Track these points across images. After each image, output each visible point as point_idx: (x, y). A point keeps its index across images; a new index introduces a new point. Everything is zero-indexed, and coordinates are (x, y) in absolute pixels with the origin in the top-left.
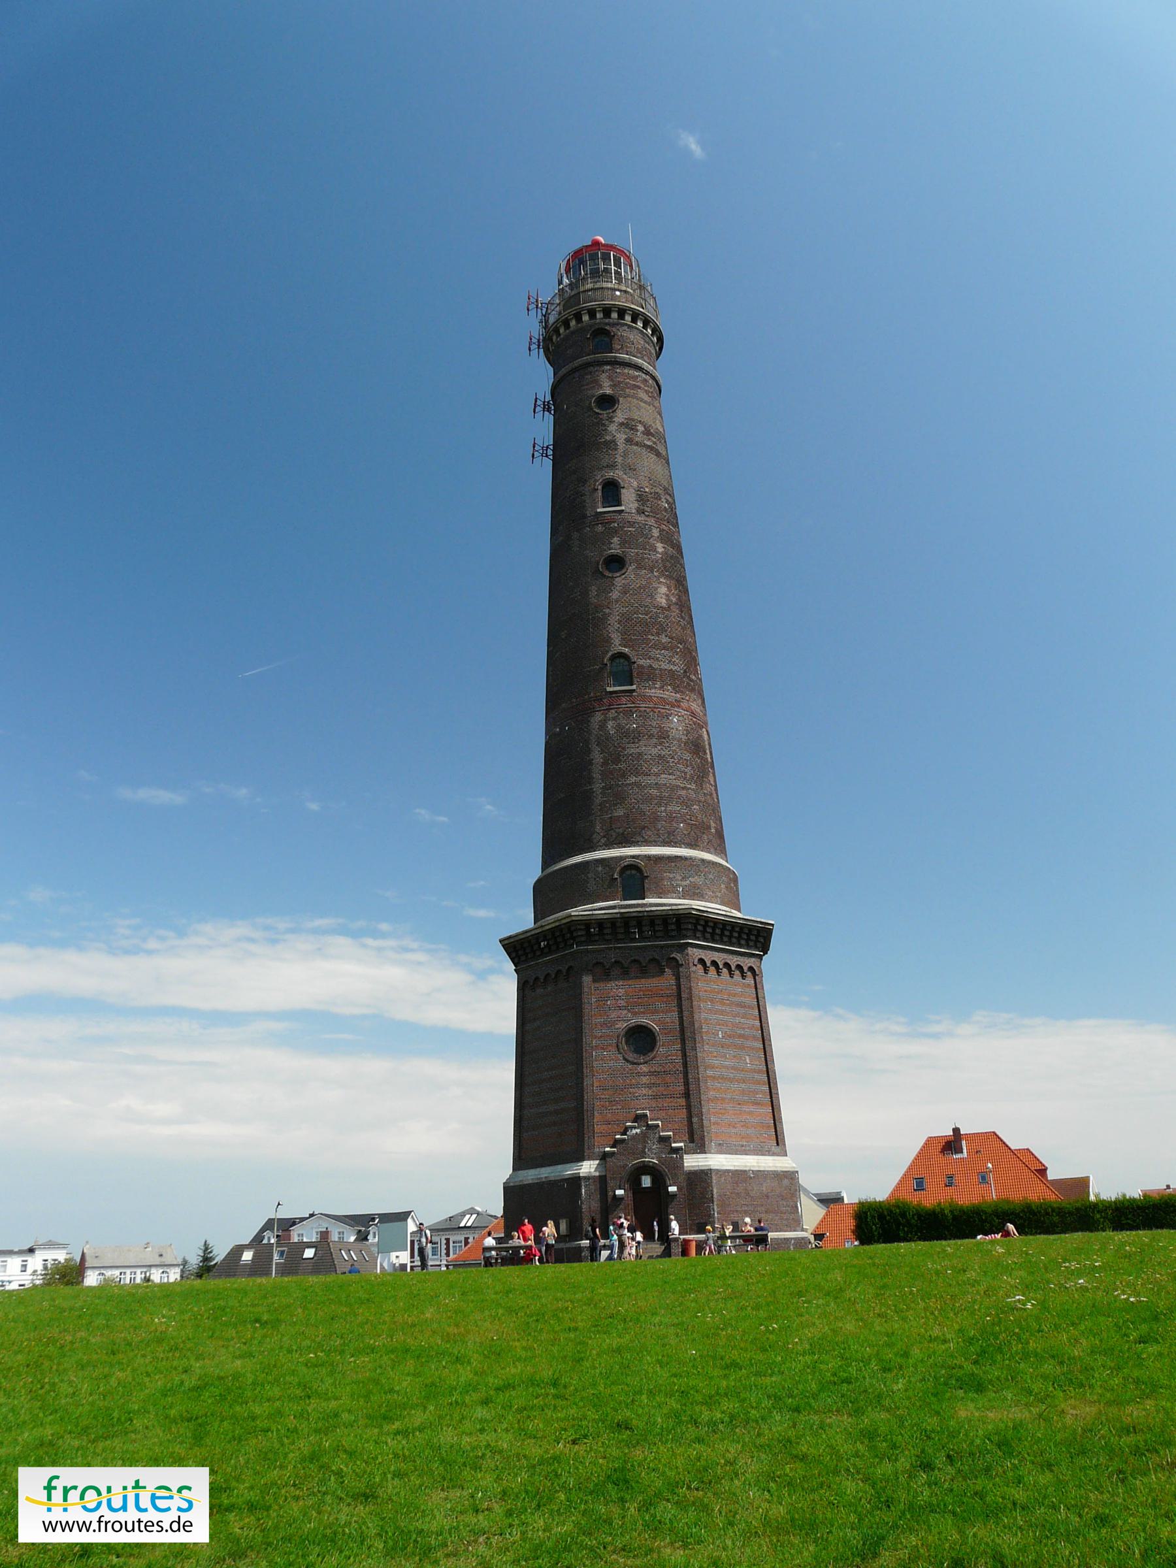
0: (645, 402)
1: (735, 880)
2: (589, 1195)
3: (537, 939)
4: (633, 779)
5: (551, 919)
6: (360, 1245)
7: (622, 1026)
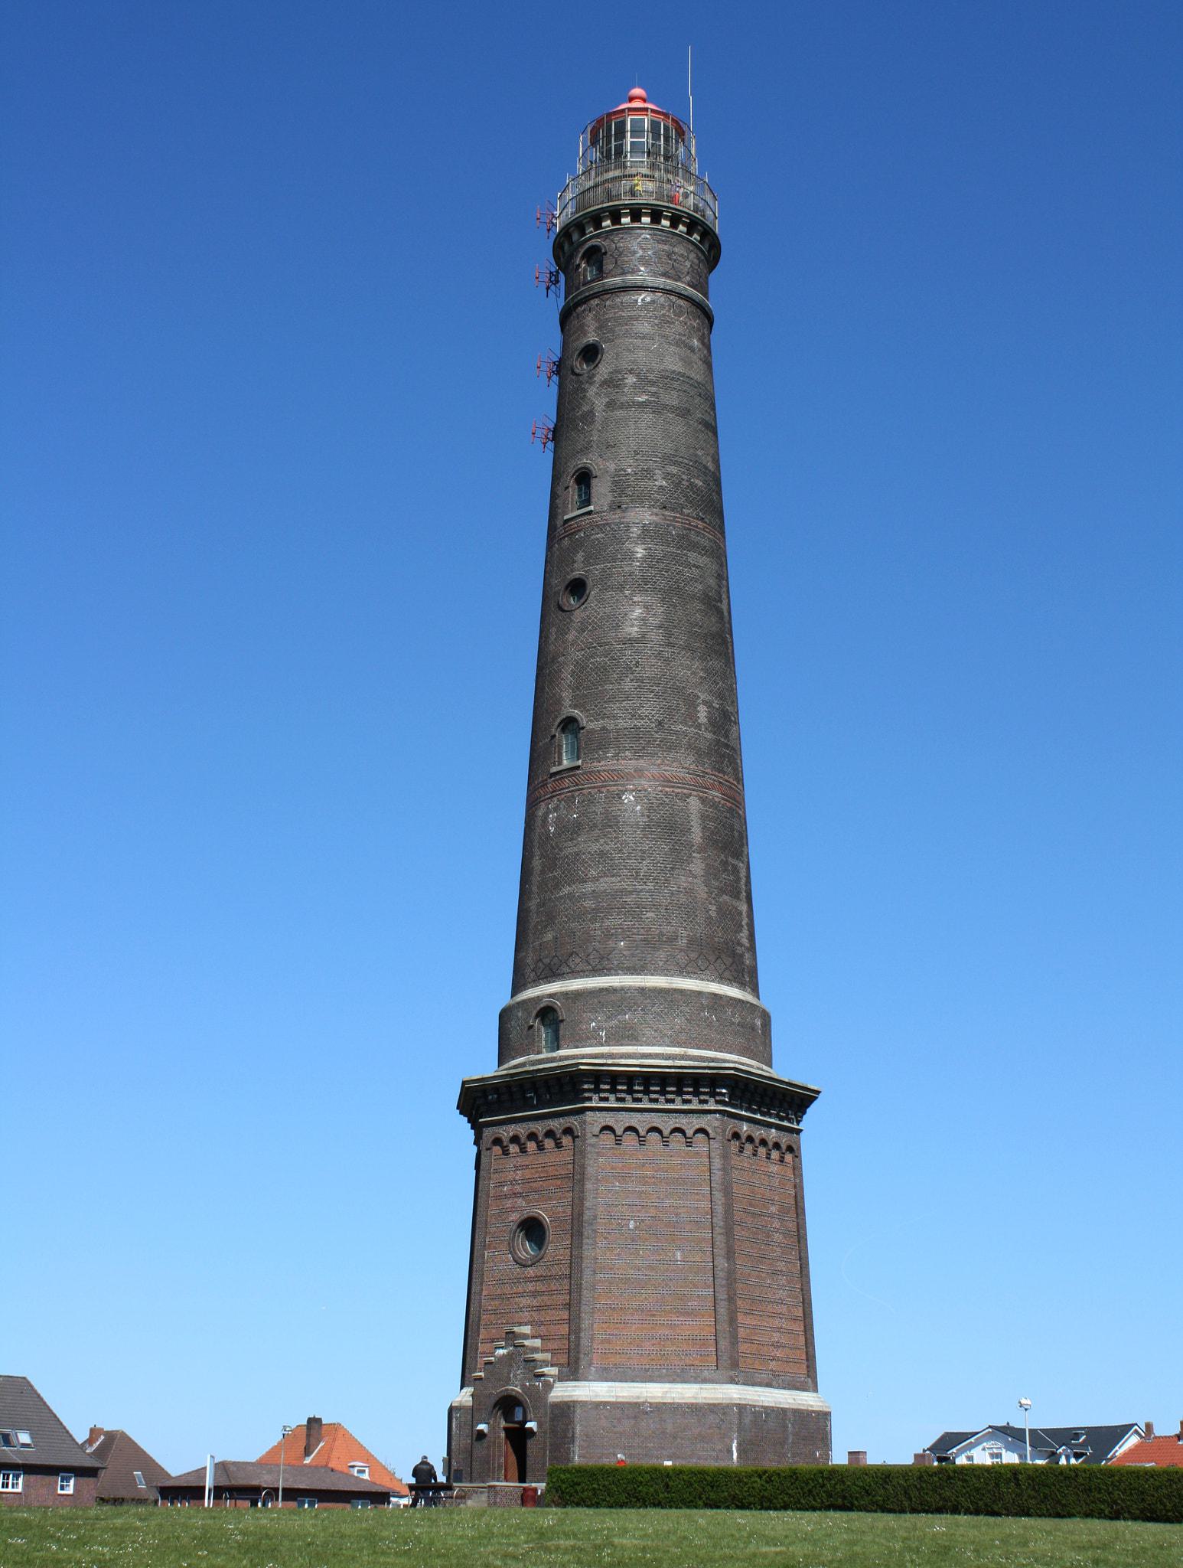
7: (515, 1217)
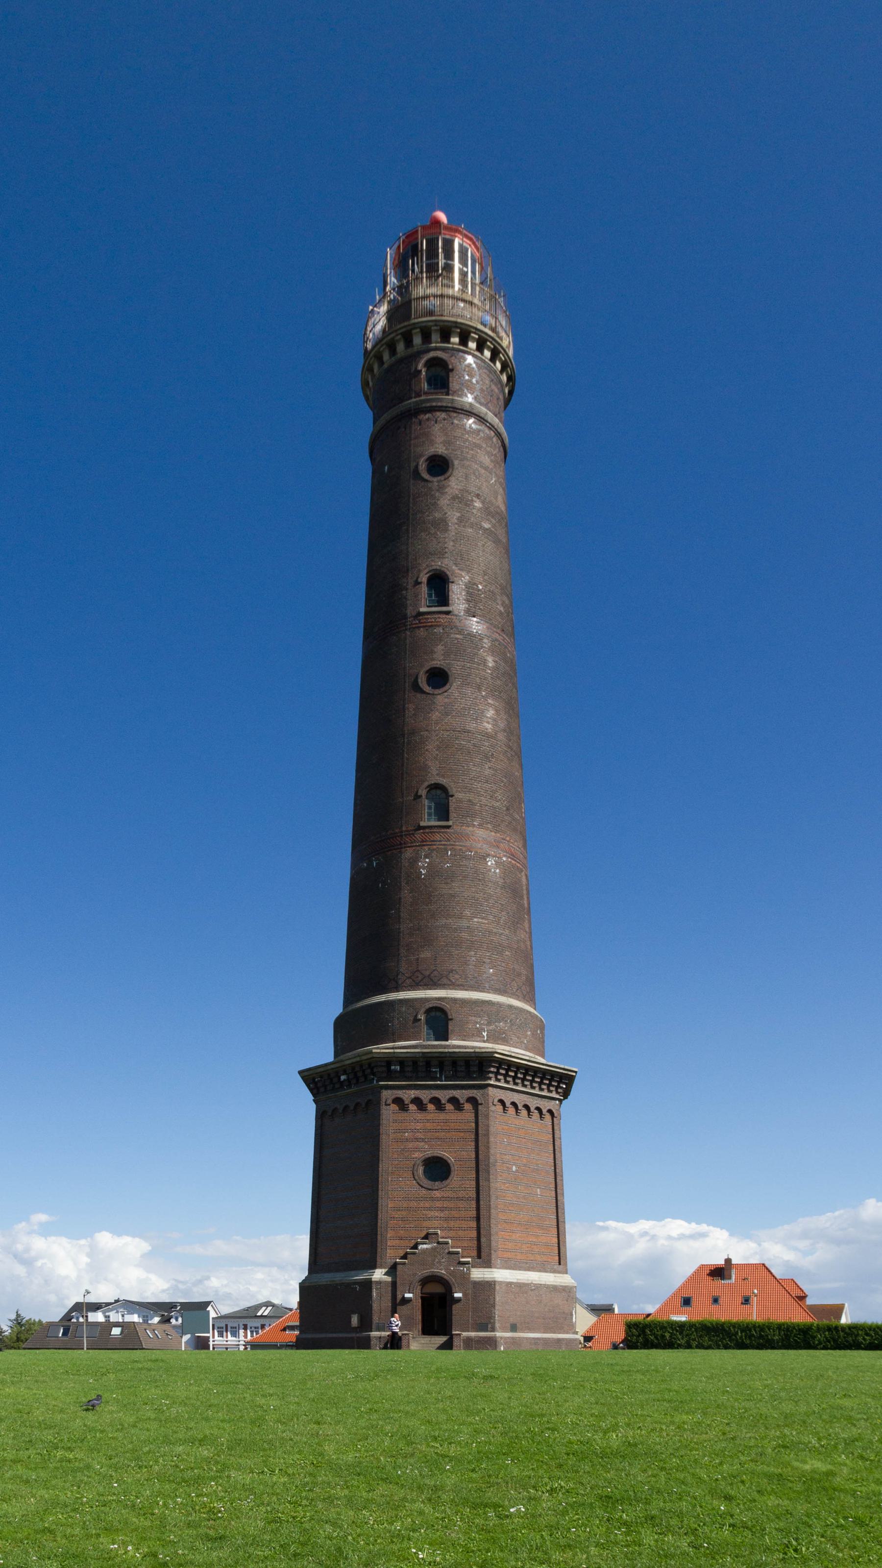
0: (486, 468)
1: (542, 1027)
2: (380, 1295)
3: (337, 1073)
5: (350, 1057)
6: (166, 1326)
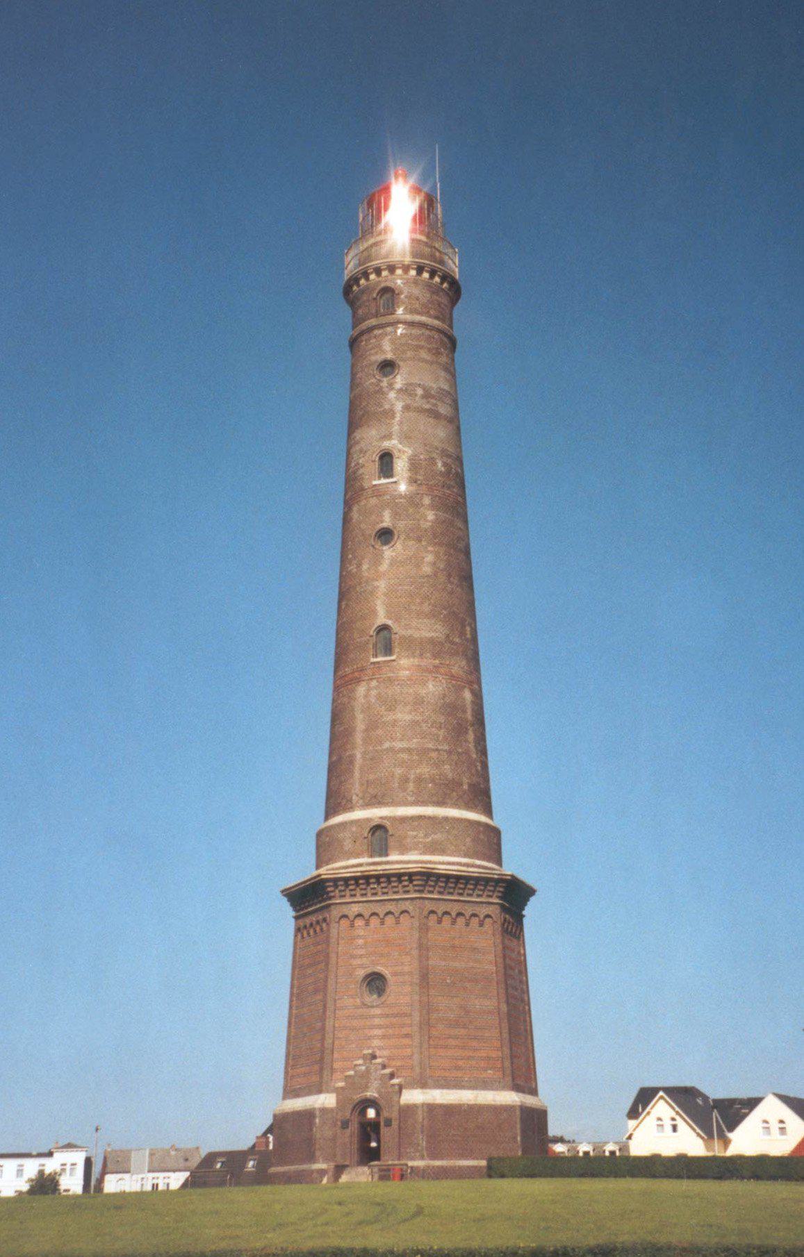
4: (387, 745)
7: (361, 973)
